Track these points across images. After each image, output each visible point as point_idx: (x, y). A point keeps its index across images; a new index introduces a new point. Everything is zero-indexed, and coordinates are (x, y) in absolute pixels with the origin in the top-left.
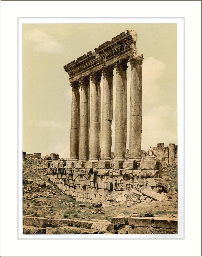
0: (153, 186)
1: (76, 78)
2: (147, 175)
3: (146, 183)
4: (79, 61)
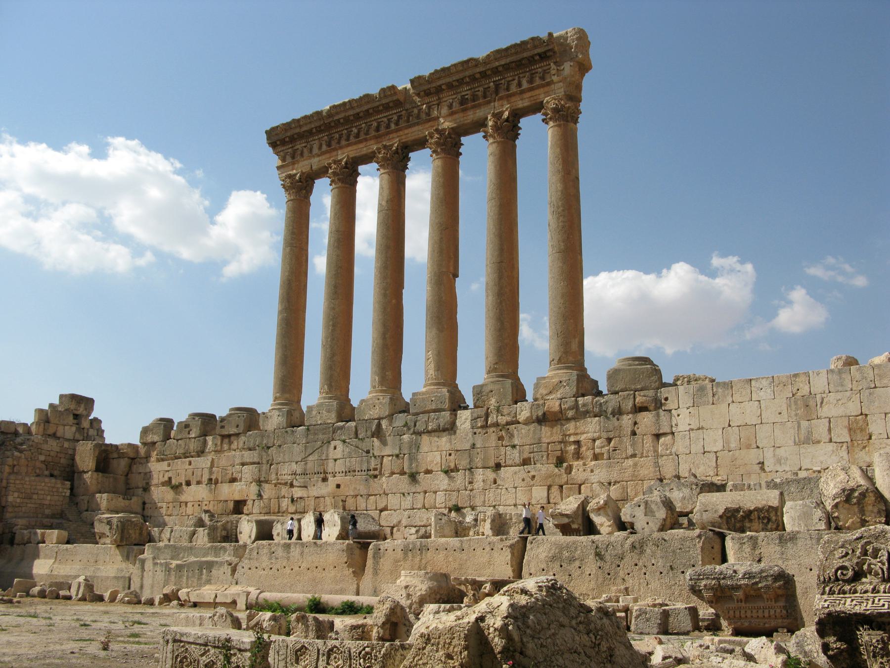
0: (661, 432)
2: (635, 405)
3: (629, 430)
4: (337, 113)
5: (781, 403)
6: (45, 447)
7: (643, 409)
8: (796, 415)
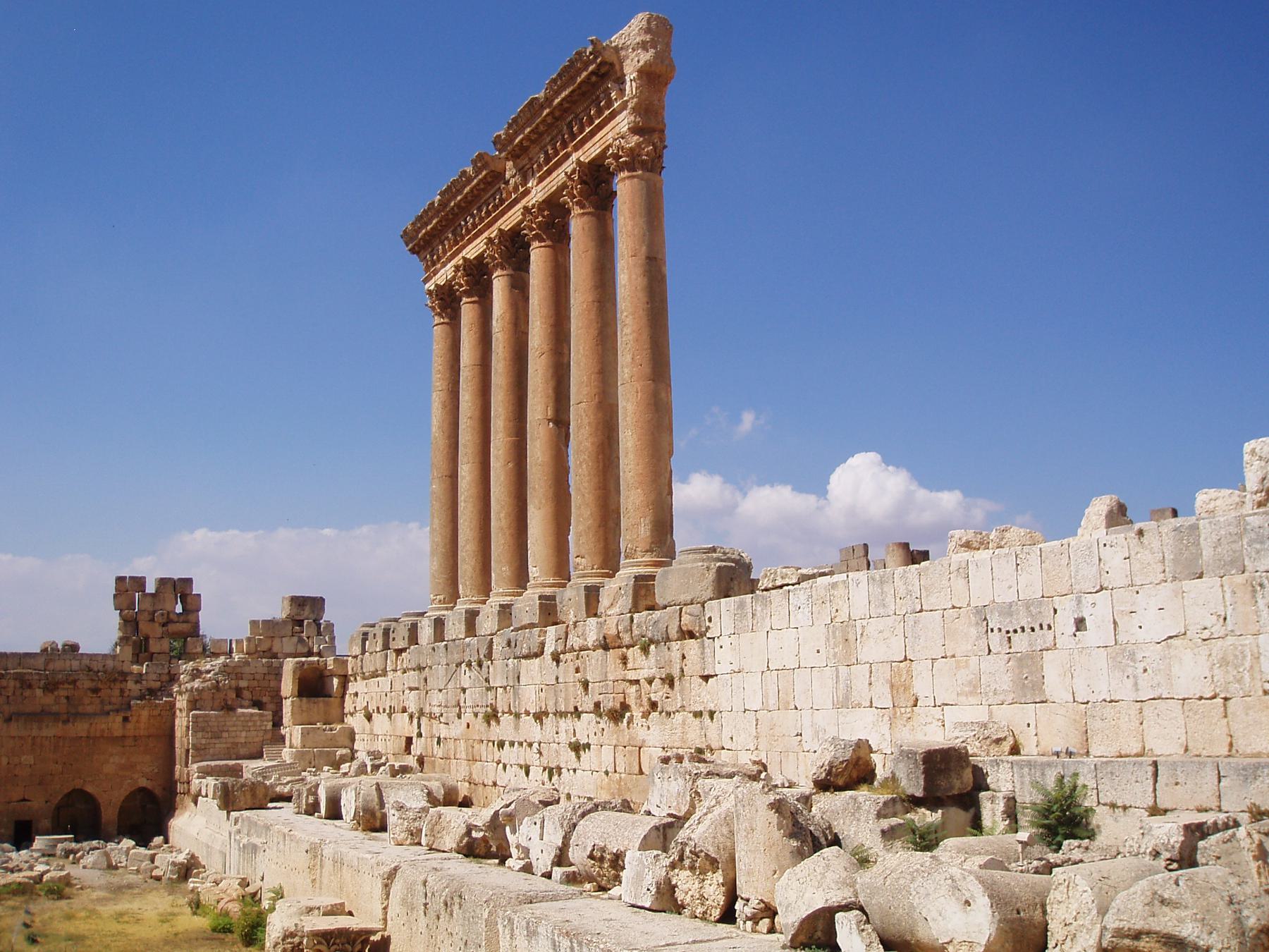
1: (445, 274)
5: (820, 630)
6: (247, 670)
7: (691, 635)
8: (835, 655)
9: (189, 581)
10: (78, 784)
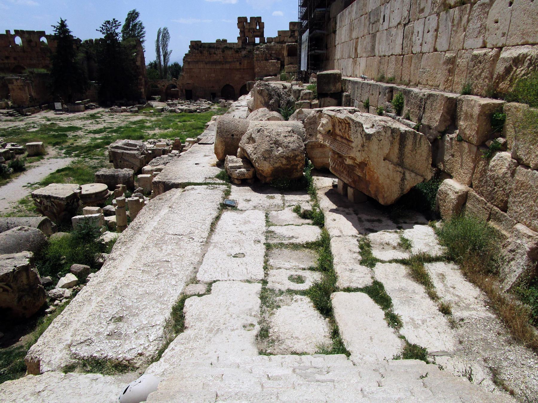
6: (274, 48)
9: (260, 18)
10: (228, 83)
